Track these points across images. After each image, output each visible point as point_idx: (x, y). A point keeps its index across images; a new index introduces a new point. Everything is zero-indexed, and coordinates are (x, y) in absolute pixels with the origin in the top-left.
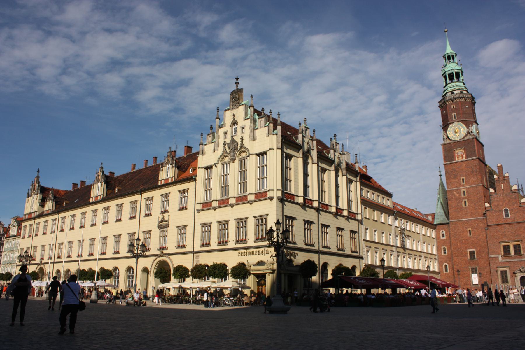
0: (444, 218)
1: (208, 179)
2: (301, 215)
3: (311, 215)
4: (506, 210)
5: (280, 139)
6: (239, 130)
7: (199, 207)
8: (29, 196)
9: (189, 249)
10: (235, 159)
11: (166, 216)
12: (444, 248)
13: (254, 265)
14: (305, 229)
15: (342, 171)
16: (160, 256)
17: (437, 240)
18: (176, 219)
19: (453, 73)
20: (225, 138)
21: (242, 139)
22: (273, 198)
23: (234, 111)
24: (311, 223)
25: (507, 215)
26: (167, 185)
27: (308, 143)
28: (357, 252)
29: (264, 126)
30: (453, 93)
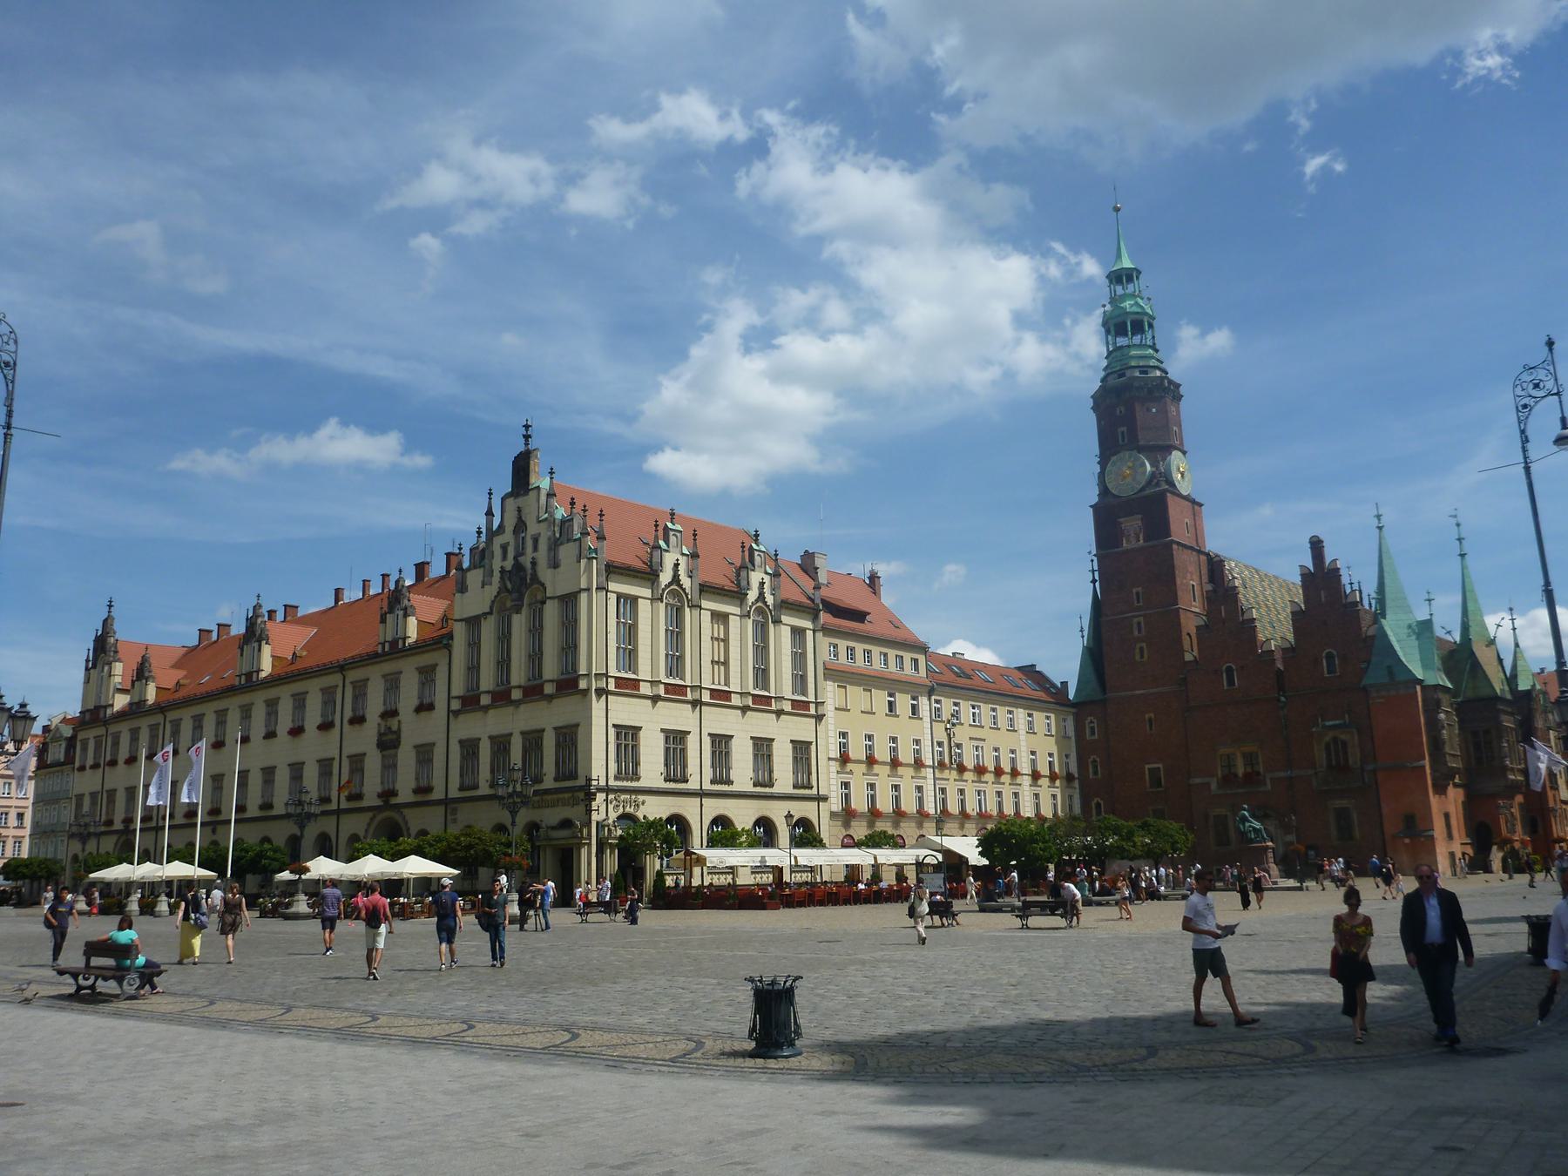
1: (474, 645)
3: (678, 716)
4: (1229, 670)
6: (529, 543)
7: (456, 705)
9: (437, 794)
13: (553, 828)
14: (667, 750)
17: (1077, 742)
18: (414, 731)
19: (1125, 324)
20: (504, 558)
21: (534, 563)
23: (521, 501)
25: (1231, 682)
27: (677, 565)
30: (1123, 375)
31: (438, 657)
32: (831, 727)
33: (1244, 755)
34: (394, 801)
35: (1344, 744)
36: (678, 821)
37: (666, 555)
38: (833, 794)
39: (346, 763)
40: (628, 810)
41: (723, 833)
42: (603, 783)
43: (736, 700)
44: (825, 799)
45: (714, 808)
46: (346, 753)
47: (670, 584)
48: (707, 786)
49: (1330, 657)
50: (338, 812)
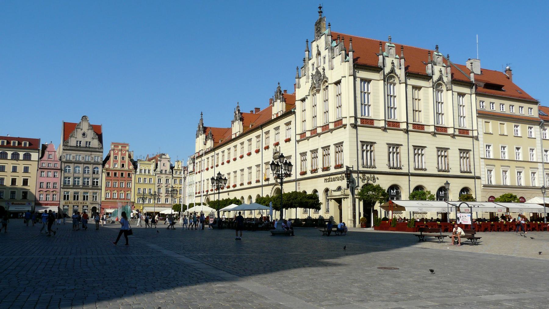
2: (382, 139)
5: (352, 65)
7: (298, 138)
8: (197, 137)
10: (320, 90)
11: (278, 147)
13: (334, 191)
14: (390, 153)
15: (446, 85)
16: (276, 185)
21: (324, 69)
22: (346, 125)
24: (398, 146)
26: (278, 118)
27: (393, 63)
28: (471, 173)
29: (338, 54)
37: (386, 58)
38: (482, 176)
40: (370, 182)
41: (418, 193)
42: (355, 169)
43: (426, 129)
44: (479, 178)
45: (416, 181)
47: (390, 73)
48: (412, 171)
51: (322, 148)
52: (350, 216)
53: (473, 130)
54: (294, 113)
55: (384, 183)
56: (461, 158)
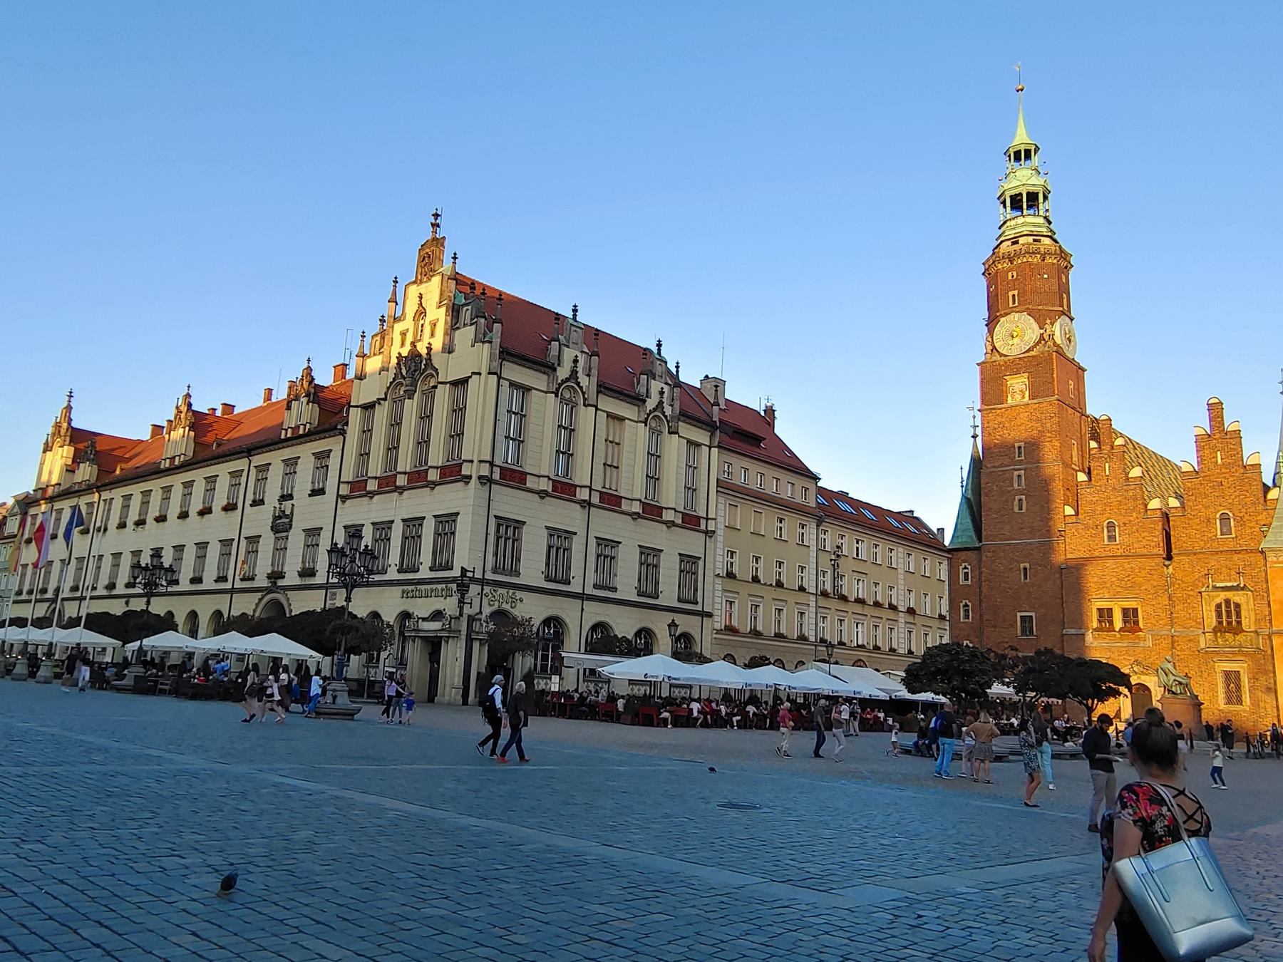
0: (970, 537)
2: (538, 517)
3: (567, 516)
4: (1111, 526)
7: (345, 490)
12: (966, 605)
13: (424, 619)
14: (550, 547)
20: (403, 344)
22: (470, 477)
26: (298, 438)
27: (576, 361)
31: (332, 443)
32: (720, 545)
33: (1125, 612)
34: (280, 583)
35: (1238, 606)
36: (554, 622)
38: (716, 613)
39: (243, 543)
40: (506, 606)
42: (478, 575)
43: (625, 506)
44: (710, 615)
45: (595, 613)
46: (245, 533)
48: (590, 590)
49: (1224, 518)
50: (232, 591)
51: (403, 520)
52: (458, 681)
53: (707, 519)
54: (343, 433)
55: (532, 610)
56: (681, 571)
